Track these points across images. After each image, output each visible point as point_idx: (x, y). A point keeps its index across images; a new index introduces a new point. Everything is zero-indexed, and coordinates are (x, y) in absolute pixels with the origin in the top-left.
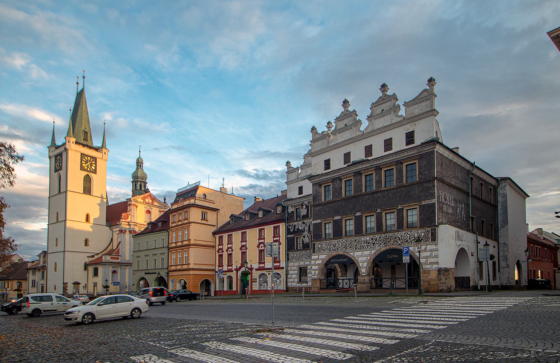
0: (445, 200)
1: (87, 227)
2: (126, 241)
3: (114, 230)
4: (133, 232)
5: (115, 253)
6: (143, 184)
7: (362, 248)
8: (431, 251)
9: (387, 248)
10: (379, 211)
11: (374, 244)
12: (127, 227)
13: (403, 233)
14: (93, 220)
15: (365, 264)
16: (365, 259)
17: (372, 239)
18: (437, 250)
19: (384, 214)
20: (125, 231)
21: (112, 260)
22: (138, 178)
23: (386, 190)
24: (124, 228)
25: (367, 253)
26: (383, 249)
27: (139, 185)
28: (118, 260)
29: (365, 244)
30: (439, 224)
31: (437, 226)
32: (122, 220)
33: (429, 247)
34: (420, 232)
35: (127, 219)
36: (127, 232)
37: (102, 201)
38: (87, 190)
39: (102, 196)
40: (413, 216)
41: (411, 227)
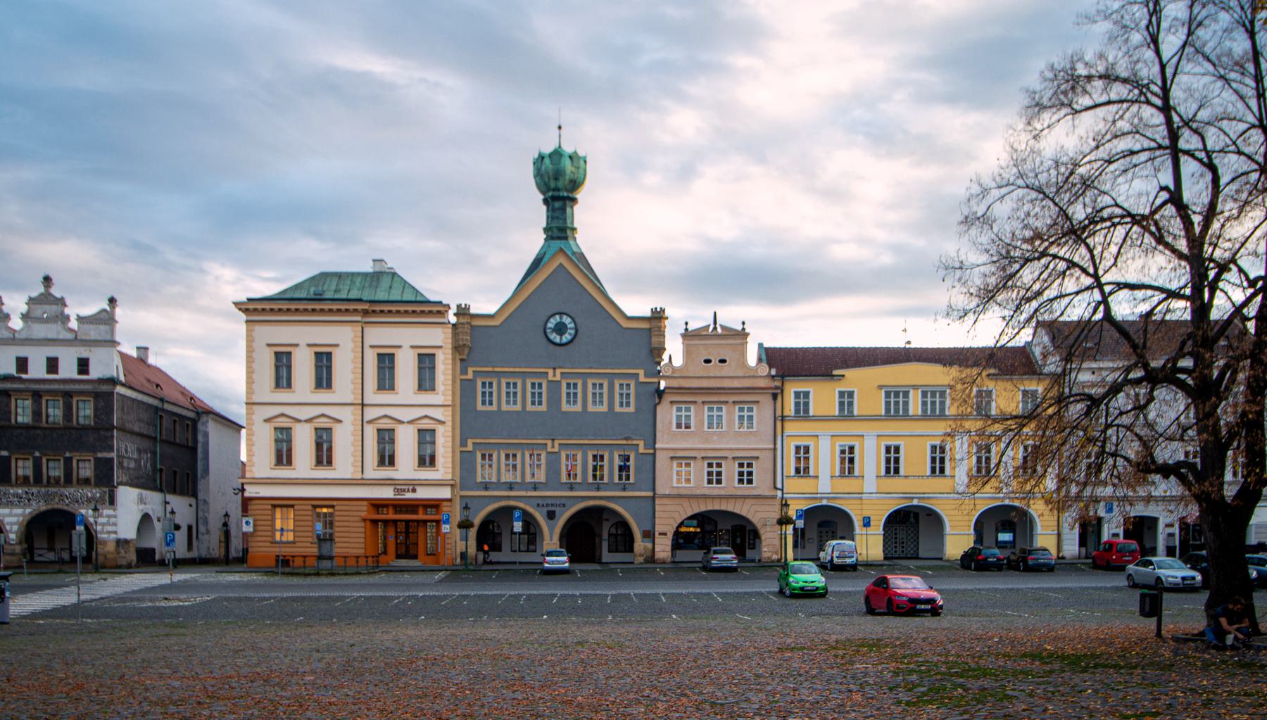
0: (126, 451)
7: (10, 504)
8: (108, 516)
9: (49, 507)
10: (37, 454)
11: (29, 500)
13: (72, 490)
15: (15, 528)
16: (14, 519)
17: (26, 493)
18: (115, 516)
19: (44, 460)
23: (50, 429)
25: (19, 511)
26: (43, 508)
29: (16, 499)
30: (119, 484)
31: (116, 487)
33: (106, 512)
34: (94, 491)
40: (87, 470)
41: (86, 482)
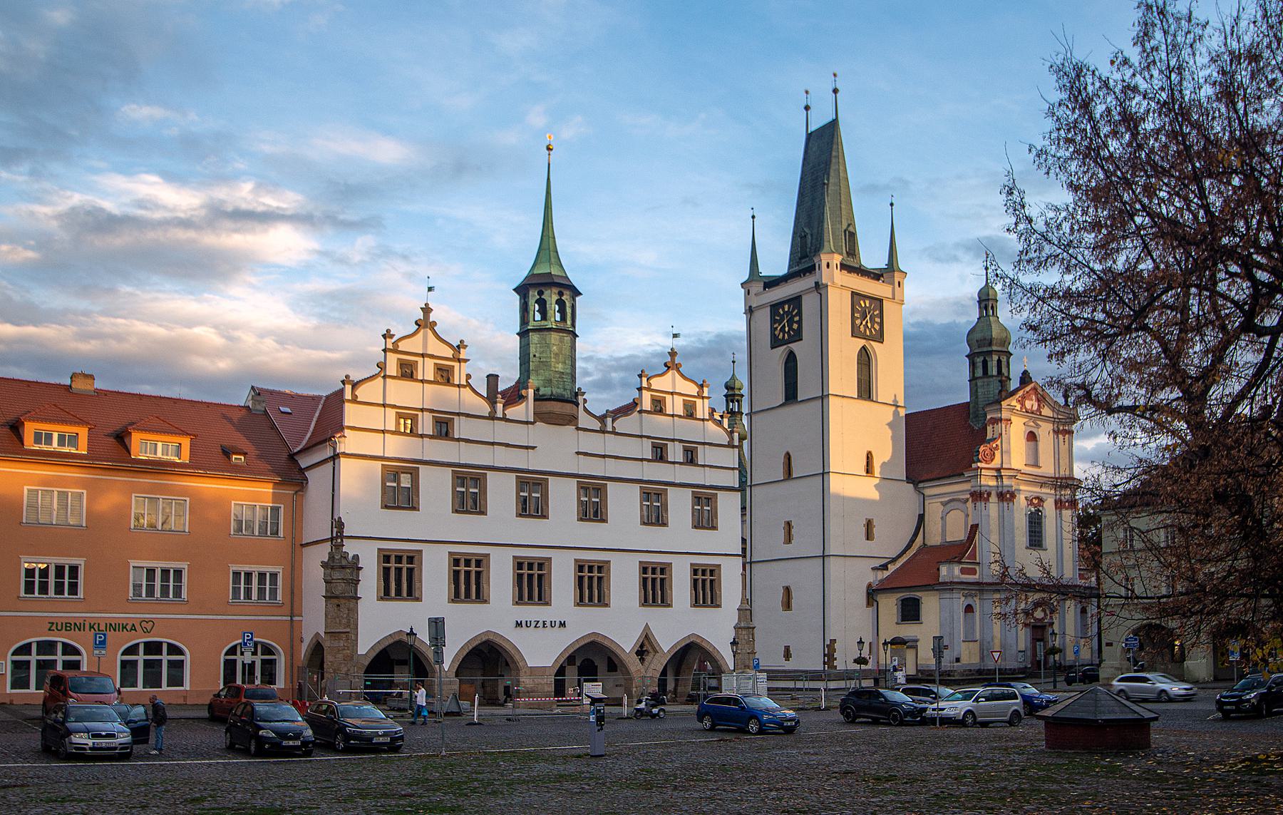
1: (867, 489)
2: (992, 522)
3: (928, 492)
4: (1008, 496)
5: (967, 558)
6: (1004, 360)
12: (993, 483)
14: (879, 470)
20: (989, 494)
21: (963, 576)
22: (990, 344)
24: (984, 486)
27: (995, 363)
28: (974, 577)
32: (979, 464)
35: (992, 461)
36: (993, 498)
37: (896, 414)
38: (866, 390)
39: (895, 400)
